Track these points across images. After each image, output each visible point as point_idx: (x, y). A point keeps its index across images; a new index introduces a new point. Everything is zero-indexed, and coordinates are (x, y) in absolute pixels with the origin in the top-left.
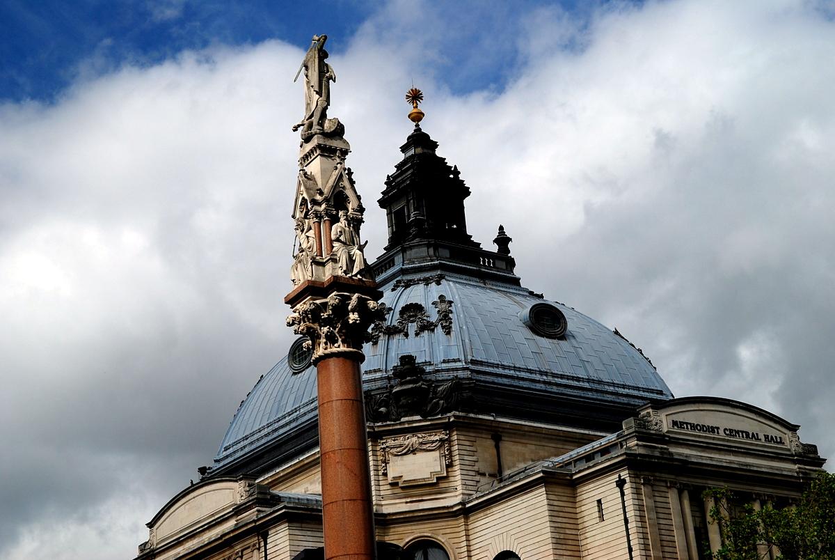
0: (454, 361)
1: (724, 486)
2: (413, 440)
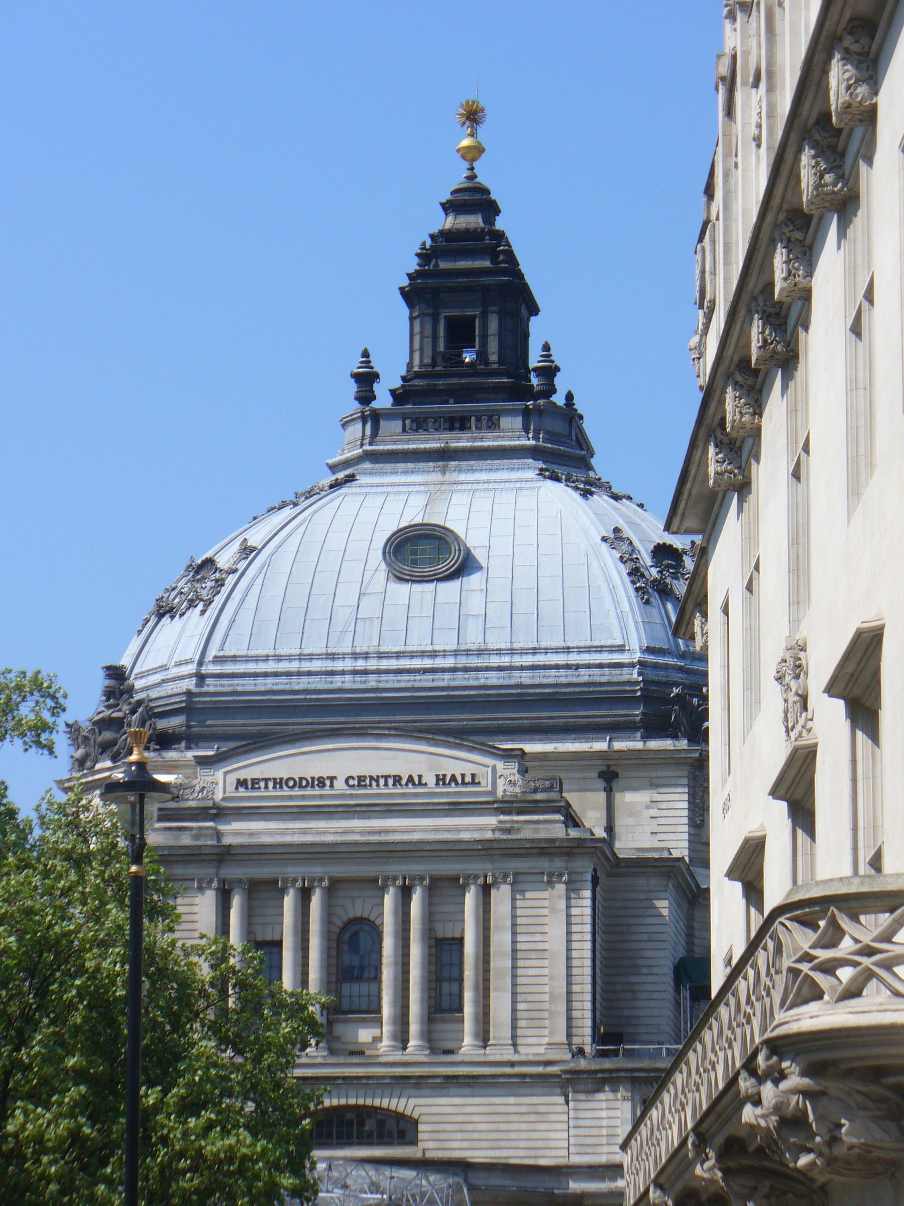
1: (316, 870)
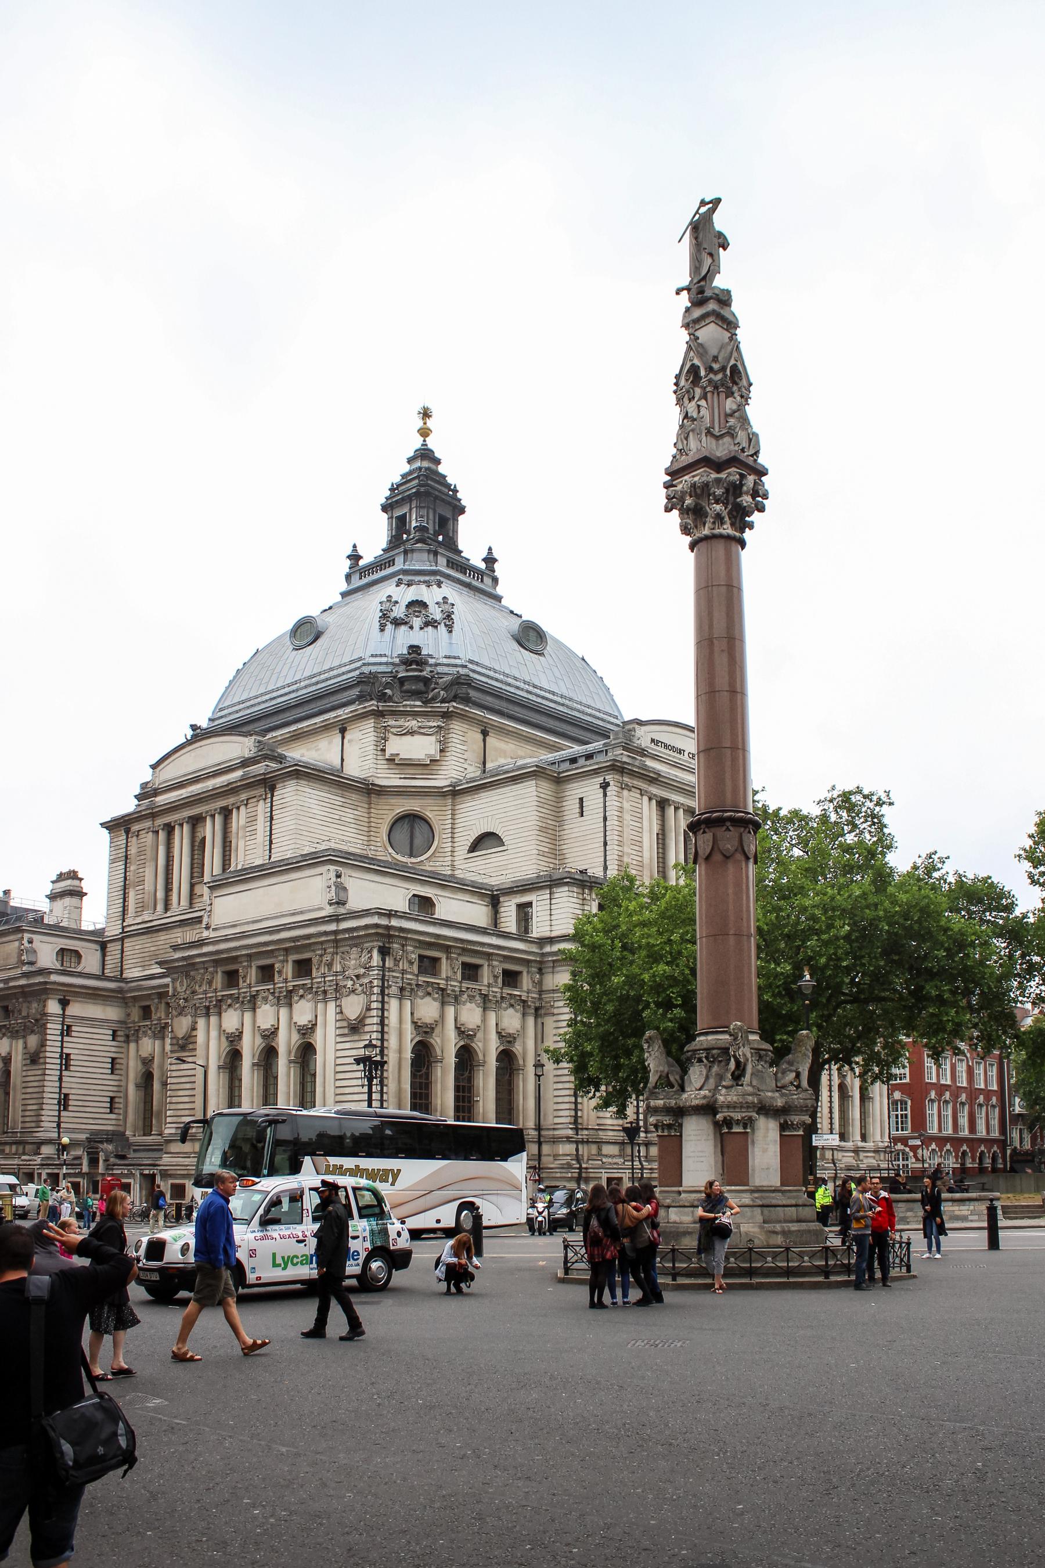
0: (455, 658)
2: (413, 724)
